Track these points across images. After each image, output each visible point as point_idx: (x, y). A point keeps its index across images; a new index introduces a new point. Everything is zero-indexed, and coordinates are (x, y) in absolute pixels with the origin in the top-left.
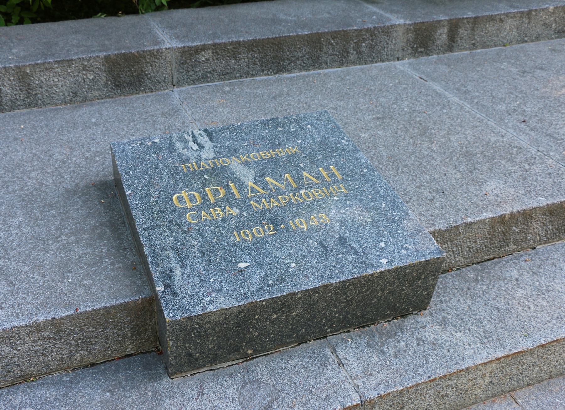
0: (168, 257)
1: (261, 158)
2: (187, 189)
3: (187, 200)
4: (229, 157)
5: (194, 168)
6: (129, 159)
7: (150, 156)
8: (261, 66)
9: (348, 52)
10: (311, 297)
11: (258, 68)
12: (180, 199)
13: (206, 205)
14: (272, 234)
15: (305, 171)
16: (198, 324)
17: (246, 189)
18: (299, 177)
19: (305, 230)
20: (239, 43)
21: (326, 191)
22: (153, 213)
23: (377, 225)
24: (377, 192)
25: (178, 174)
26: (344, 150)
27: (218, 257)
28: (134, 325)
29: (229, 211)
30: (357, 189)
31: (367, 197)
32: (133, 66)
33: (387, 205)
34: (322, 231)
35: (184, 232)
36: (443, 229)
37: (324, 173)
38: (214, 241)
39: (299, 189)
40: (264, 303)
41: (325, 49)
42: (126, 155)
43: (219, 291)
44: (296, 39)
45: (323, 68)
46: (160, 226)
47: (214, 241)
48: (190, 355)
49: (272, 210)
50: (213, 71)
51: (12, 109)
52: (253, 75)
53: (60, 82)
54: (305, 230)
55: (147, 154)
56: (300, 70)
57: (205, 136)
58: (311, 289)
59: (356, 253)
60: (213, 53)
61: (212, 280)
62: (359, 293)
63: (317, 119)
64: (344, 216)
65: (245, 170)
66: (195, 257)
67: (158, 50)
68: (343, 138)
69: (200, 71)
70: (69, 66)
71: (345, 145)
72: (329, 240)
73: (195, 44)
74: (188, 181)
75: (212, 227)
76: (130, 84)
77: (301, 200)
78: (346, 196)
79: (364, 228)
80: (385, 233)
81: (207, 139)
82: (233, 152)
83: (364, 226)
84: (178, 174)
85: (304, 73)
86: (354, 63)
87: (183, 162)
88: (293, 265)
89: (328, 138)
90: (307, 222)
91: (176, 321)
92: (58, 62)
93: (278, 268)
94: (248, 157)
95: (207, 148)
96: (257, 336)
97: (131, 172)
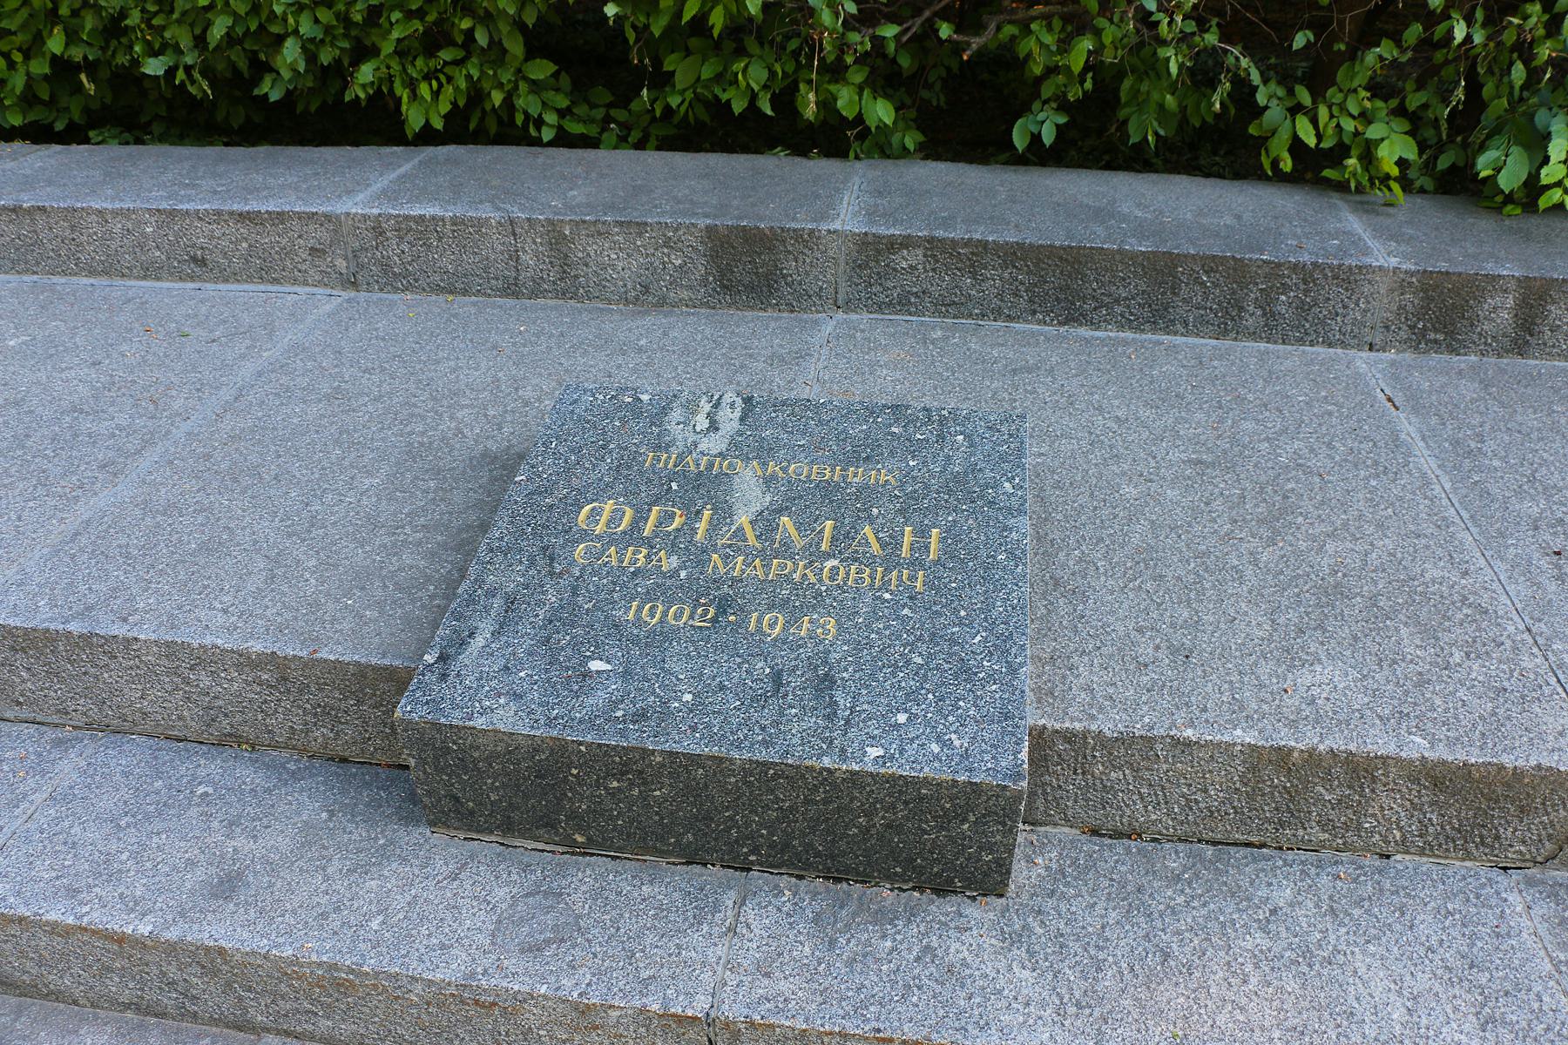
0: (487, 610)
3: (604, 519)
8: (1031, 301)
9: (1241, 309)
11: (1023, 304)
13: (633, 536)
20: (984, 244)
21: (879, 576)
24: (988, 607)
25: (629, 468)
29: (660, 560)
32: (759, 255)
33: (985, 639)
35: (551, 574)
36: (1108, 734)
39: (828, 556)
41: (1184, 291)
43: (517, 697)
44: (1118, 257)
45: (1176, 333)
48: (457, 799)
51: (534, 295)
52: (1010, 318)
53: (621, 262)
56: (1121, 327)
59: (830, 717)
61: (522, 674)
62: (807, 801)
67: (812, 231)
68: (1010, 480)
70: (640, 235)
73: (891, 232)
76: (751, 288)
77: (813, 580)
78: (911, 598)
79: (894, 674)
80: (930, 696)
81: (738, 414)
82: (764, 451)
84: (629, 468)
85: (1129, 335)
86: (1254, 336)
87: (657, 448)
88: (688, 697)
90: (788, 624)
91: (410, 722)
92: (621, 224)
93: (653, 693)
94: (784, 470)
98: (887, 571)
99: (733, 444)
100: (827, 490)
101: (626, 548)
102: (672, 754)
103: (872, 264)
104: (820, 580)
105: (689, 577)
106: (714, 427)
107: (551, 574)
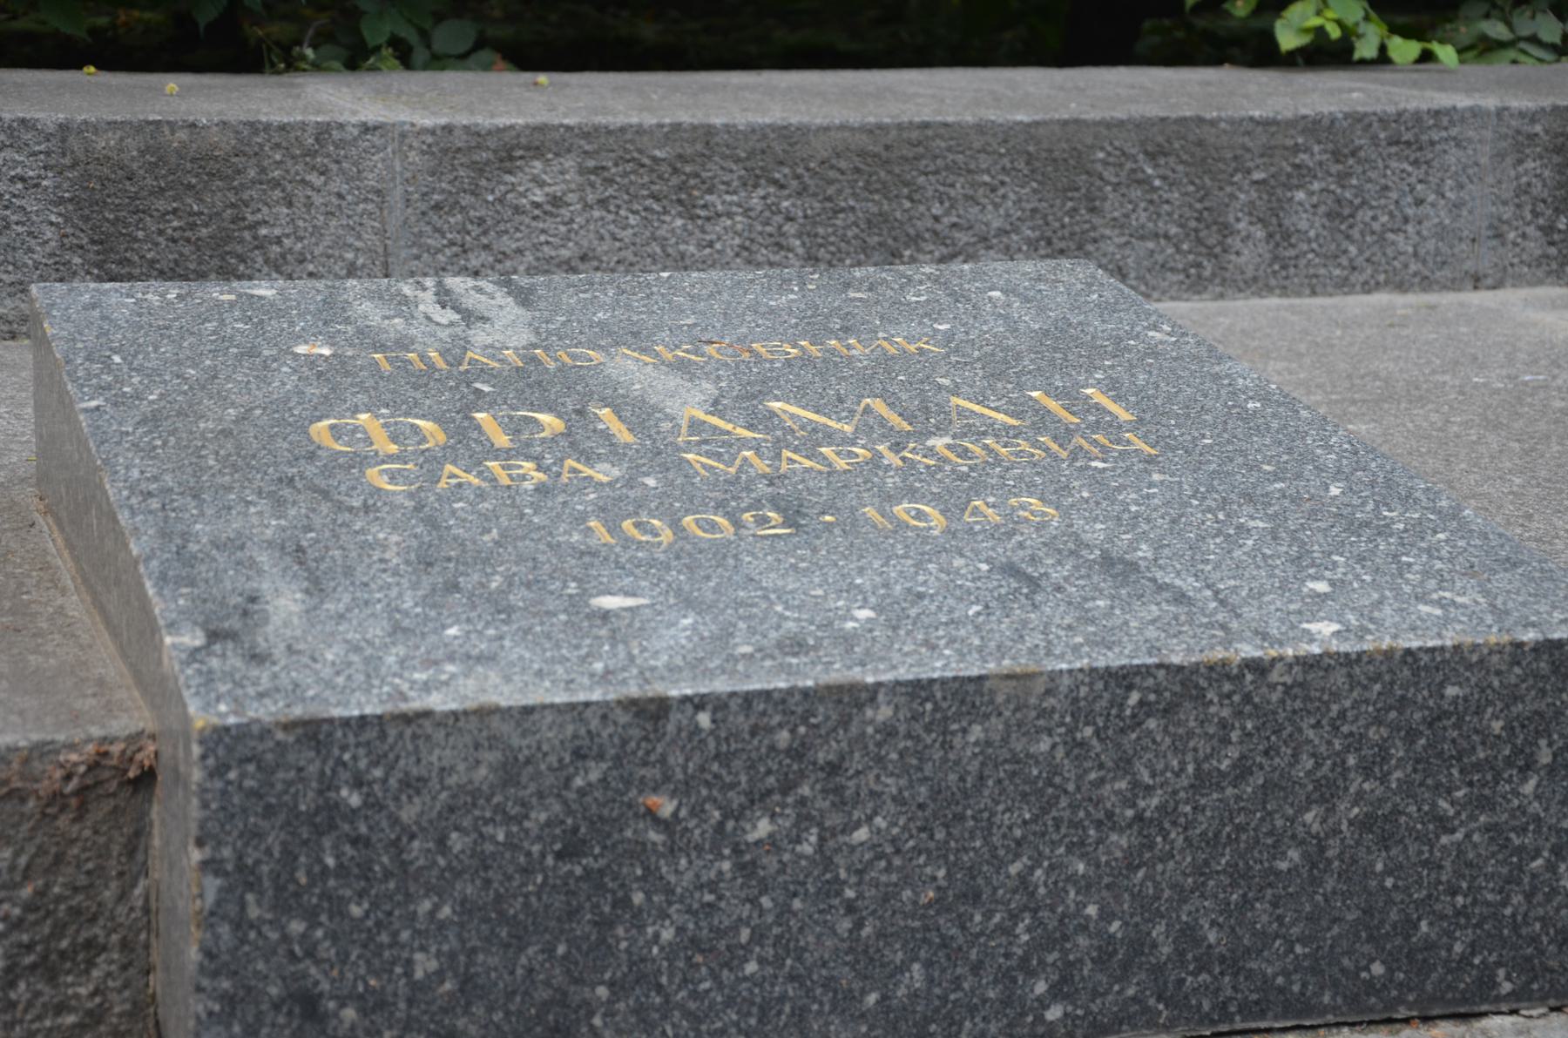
9: (1226, 230)
10: (947, 746)
16: (358, 783)
28: (29, 907)
40: (704, 719)
41: (1113, 205)
50: (583, 258)
58: (943, 682)
60: (582, 171)
62: (1203, 781)
69: (519, 251)
86: (1256, 285)
96: (671, 952)
102: (918, 689)
103: (466, 200)
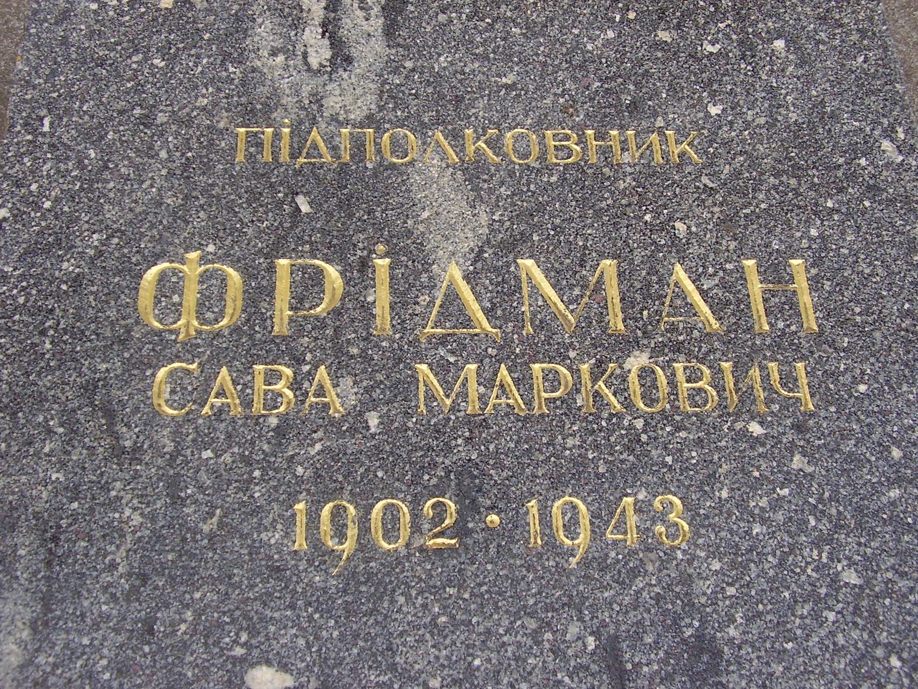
1: (542, 157)
2: (211, 248)
3: (191, 298)
4: (421, 129)
5: (275, 154)
6: (68, 59)
7: (146, 59)
12: (168, 286)
14: (439, 551)
15: (682, 260)
17: (424, 299)
18: (649, 285)
19: (574, 561)
22: (43, 333)
23: (873, 613)
25: (207, 168)
26: (873, 190)
27: (189, 615)
29: (321, 392)
30: (860, 399)
31: (883, 449)
34: (639, 583)
35: (118, 452)
37: (756, 287)
38: (206, 528)
39: (628, 345)
42: (64, 41)
46: (42, 399)
47: (206, 528)
49: (485, 424)
54: (574, 561)
55: (137, 51)
57: (376, 10)
63: (823, 19)
64: (757, 529)
65: (458, 206)
66: (105, 589)
68: (889, 133)
71: (888, 165)
72: (649, 639)
74: (231, 209)
75: (227, 458)
78: (799, 428)
79: (816, 615)
80: (895, 662)
81: (377, 24)
82: (447, 107)
83: (818, 600)
87: (249, 115)
89: (832, 116)
90: (599, 520)
94: (495, 144)
95: (359, 68)
97: (47, 122)
98: (740, 370)
99: (389, 96)
100: (585, 181)
101: (248, 369)
104: (628, 404)
105: (386, 422)
106: (341, 57)
107: (118, 452)
